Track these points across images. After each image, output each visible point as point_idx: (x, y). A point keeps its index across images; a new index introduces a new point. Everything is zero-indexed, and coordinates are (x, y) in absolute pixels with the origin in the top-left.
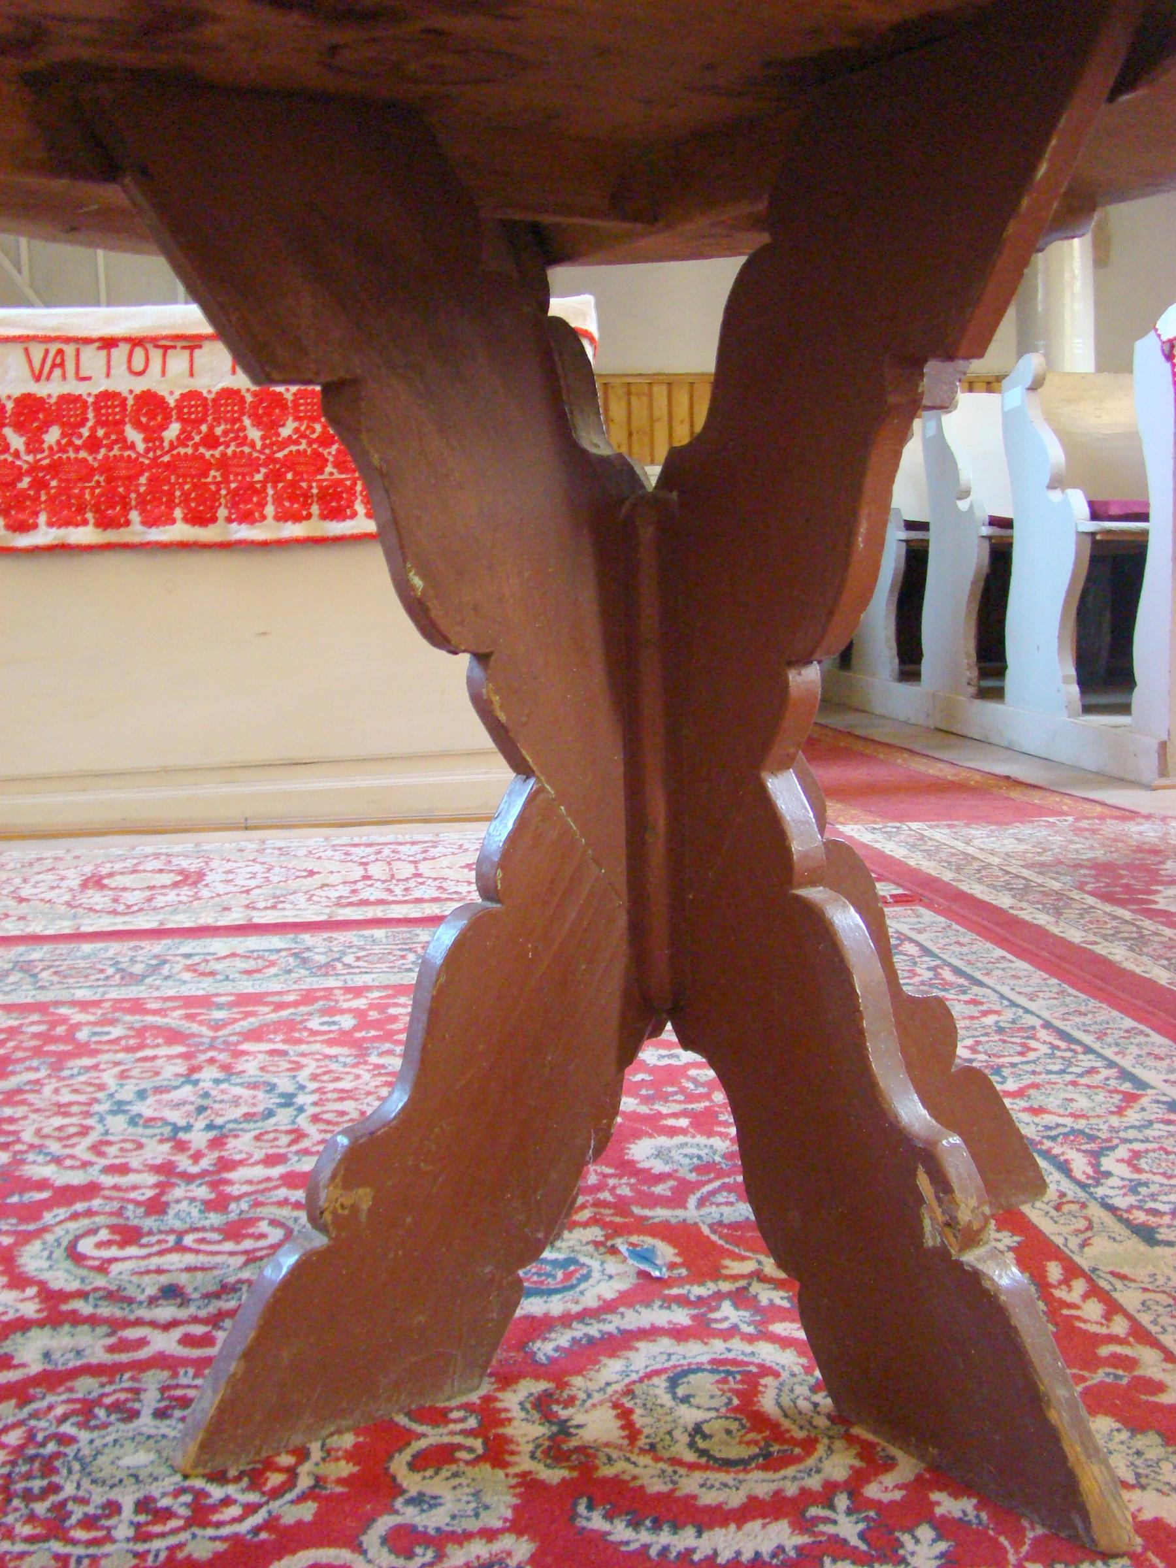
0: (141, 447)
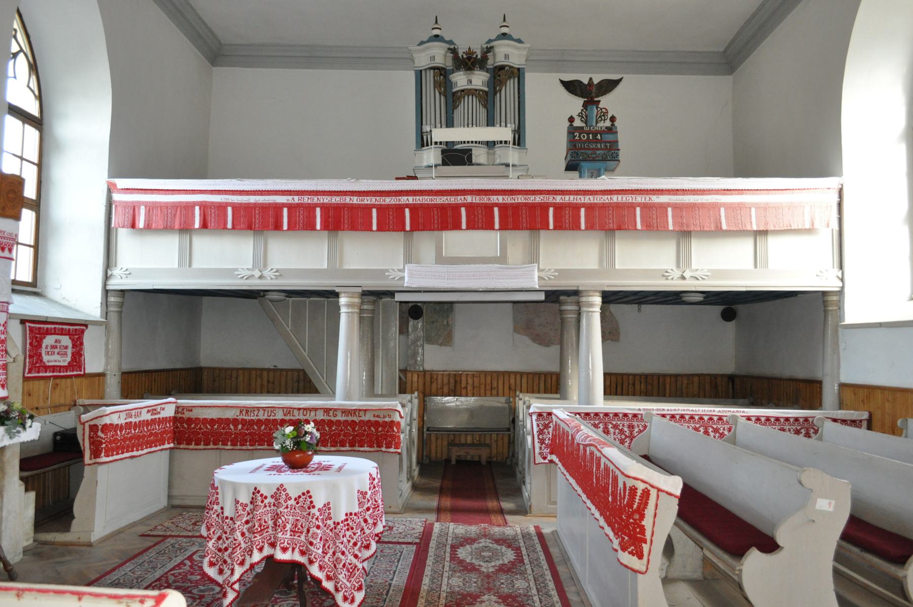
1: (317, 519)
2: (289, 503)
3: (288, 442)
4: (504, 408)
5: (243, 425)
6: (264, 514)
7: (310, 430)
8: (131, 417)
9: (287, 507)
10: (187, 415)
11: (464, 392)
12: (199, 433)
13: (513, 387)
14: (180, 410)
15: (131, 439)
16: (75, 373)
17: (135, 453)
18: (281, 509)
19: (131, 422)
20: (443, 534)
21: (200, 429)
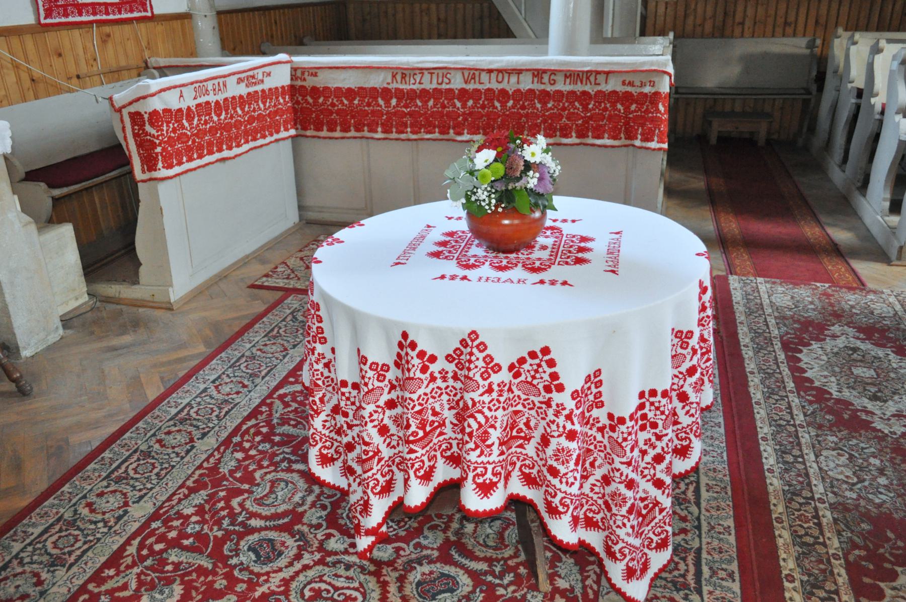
0: (499, 108)
1: (569, 417)
2: (495, 379)
3: (482, 195)
4: (804, 56)
5: (399, 100)
6: (430, 396)
7: (537, 159)
8: (207, 92)
9: (490, 390)
10: (310, 82)
11: (738, 31)
12: (331, 113)
13: (822, 20)
14: (299, 74)
15: (213, 131)
16: (136, 14)
17: (226, 153)
18: (475, 396)
19: (208, 103)
20: (755, 309)
21: (333, 105)
